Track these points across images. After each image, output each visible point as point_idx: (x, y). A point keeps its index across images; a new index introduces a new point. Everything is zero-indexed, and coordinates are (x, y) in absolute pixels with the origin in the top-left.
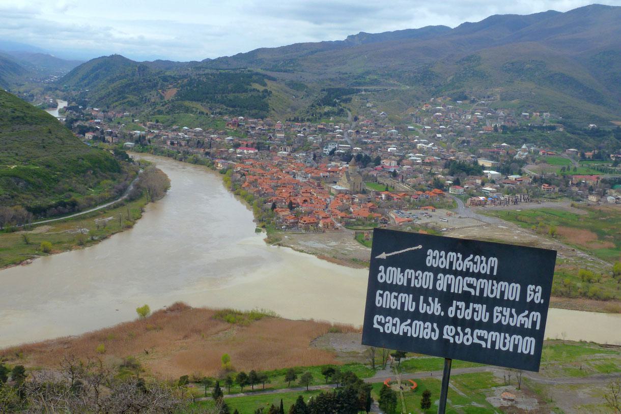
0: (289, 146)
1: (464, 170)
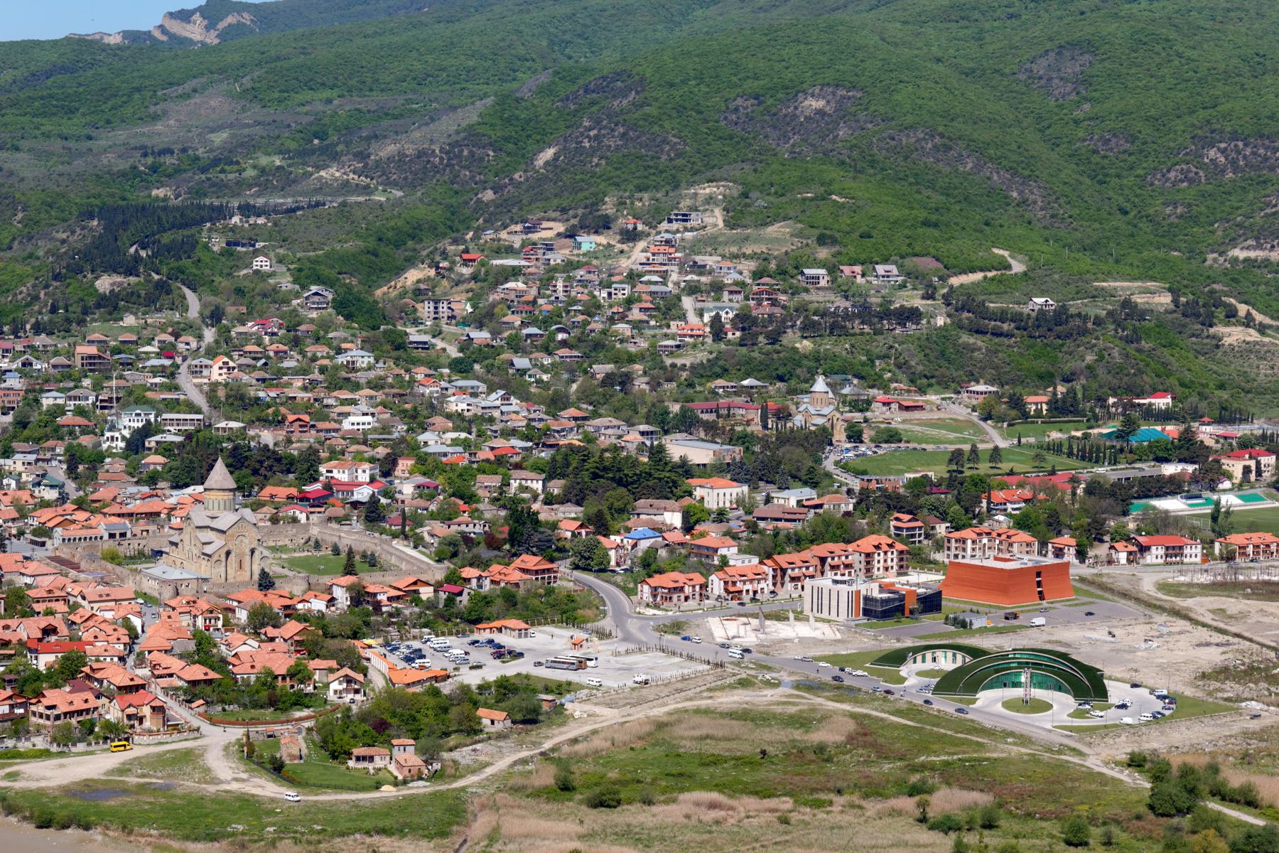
1: (620, 482)
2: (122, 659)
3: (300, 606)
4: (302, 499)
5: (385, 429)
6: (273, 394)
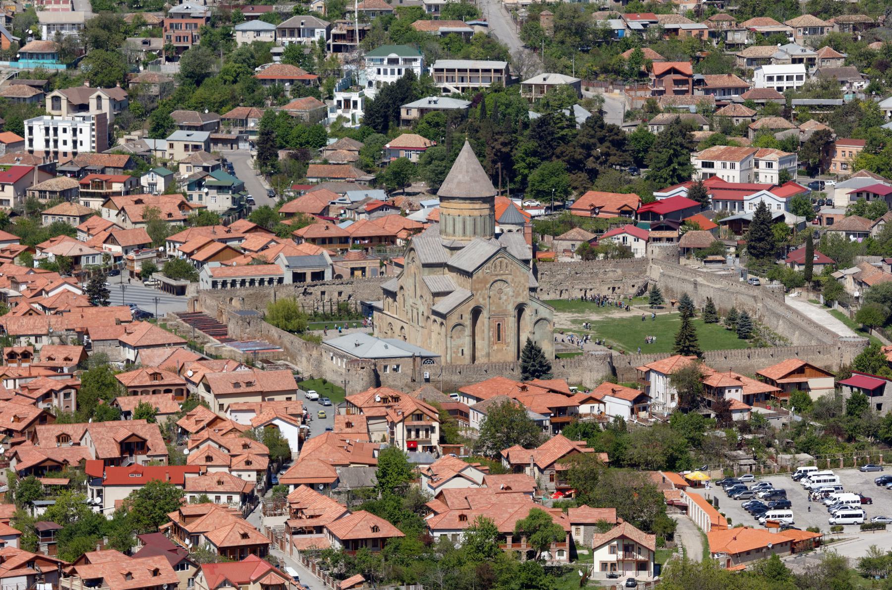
0: (110, 85)
2: (249, 498)
3: (584, 409)
4: (645, 216)
5: (829, 87)
6: (636, 25)
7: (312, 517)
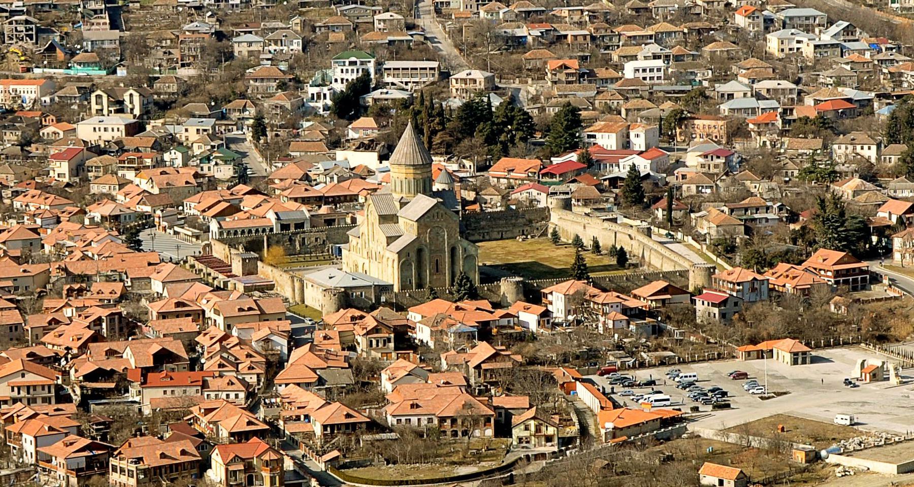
7: (299, 408)
